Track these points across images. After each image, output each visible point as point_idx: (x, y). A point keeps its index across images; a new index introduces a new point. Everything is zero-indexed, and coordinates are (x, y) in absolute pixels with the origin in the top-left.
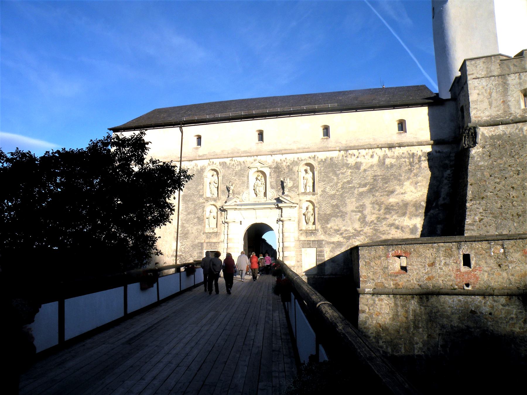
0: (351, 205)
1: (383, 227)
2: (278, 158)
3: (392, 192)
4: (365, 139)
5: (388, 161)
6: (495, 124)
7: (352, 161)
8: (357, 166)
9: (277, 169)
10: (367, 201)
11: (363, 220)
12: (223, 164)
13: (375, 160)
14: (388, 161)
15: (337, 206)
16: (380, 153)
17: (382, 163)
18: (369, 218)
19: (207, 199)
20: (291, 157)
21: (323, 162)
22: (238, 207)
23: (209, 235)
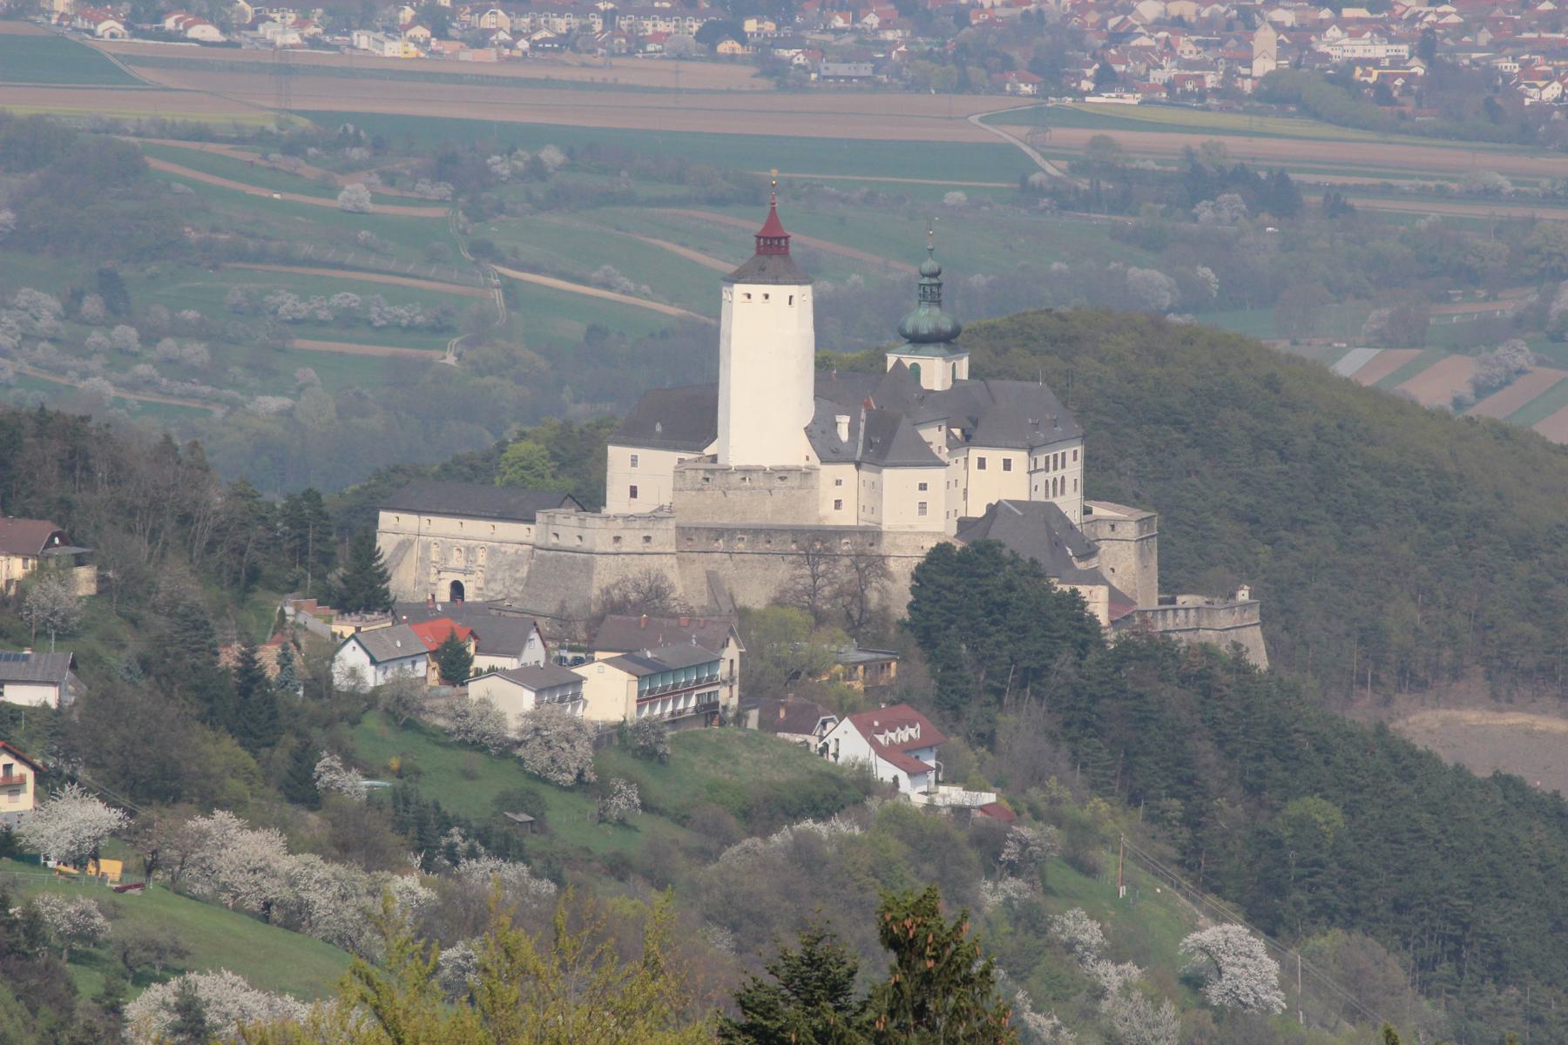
0: (499, 576)
1: (511, 591)
2: (469, 542)
3: (518, 571)
4: (511, 537)
5: (520, 552)
6: (541, 549)
7: (503, 549)
8: (505, 553)
9: (468, 548)
10: (507, 574)
11: (504, 584)
12: (441, 541)
13: (513, 551)
14: (520, 552)
15: (493, 575)
16: (517, 546)
17: (516, 552)
18: (507, 584)
19: (432, 562)
20: (475, 543)
21: (490, 547)
22: (446, 570)
23: (432, 584)
